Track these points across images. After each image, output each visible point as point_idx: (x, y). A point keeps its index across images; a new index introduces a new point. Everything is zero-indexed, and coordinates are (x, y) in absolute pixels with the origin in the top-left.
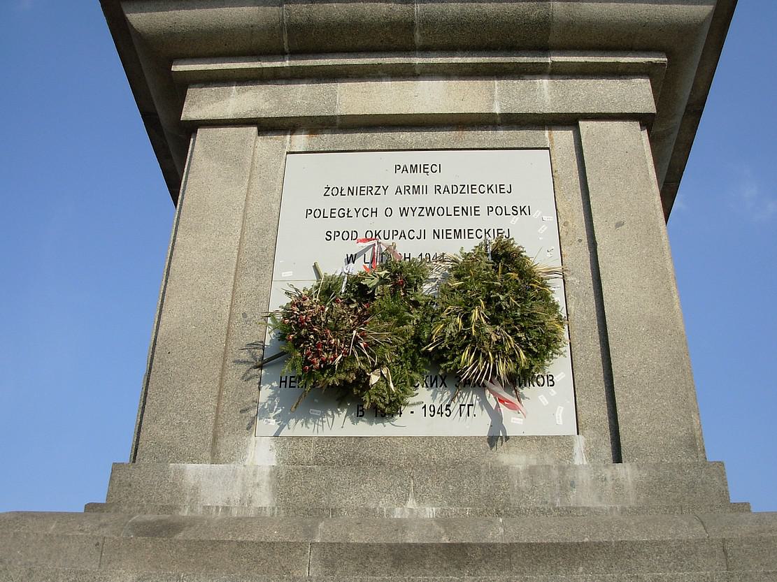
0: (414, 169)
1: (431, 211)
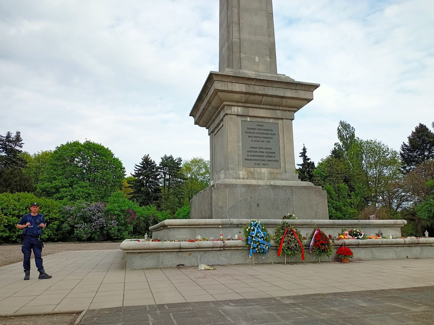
1: (262, 133)
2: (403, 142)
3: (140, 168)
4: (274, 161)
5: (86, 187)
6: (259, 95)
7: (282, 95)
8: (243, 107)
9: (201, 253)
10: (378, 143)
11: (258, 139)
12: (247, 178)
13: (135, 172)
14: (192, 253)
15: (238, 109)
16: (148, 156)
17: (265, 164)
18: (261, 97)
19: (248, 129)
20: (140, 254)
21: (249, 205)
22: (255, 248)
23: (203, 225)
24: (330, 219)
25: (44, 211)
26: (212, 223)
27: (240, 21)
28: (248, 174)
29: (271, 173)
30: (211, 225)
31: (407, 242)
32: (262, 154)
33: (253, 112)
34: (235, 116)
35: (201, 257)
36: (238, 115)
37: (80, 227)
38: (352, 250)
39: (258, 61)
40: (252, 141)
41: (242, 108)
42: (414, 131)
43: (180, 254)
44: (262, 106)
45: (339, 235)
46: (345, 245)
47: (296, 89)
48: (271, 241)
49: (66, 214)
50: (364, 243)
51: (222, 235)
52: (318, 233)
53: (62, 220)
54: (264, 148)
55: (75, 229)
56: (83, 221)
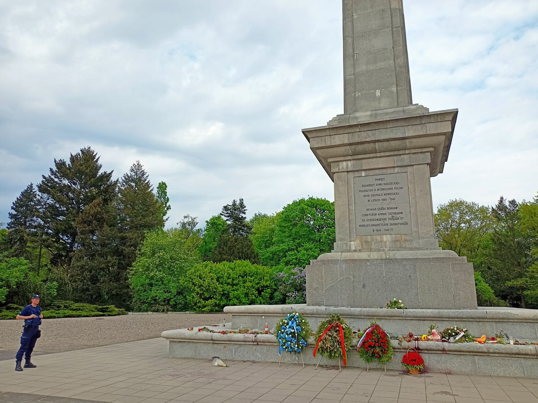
0: (379, 179)
5: (311, 249)
6: (369, 142)
8: (355, 161)
9: (236, 347)
11: (376, 198)
12: (359, 250)
14: (227, 345)
15: (347, 165)
17: (388, 230)
18: (372, 145)
20: (180, 343)
21: (351, 286)
23: (264, 313)
24: (480, 304)
25: (256, 278)
26: (271, 312)
27: (355, 51)
28: (362, 245)
30: (271, 313)
32: (384, 217)
34: (344, 173)
35: (236, 351)
36: (348, 172)
37: (291, 296)
38: (425, 357)
39: (380, 95)
40: (369, 201)
41: (352, 162)
43: (215, 345)
44: (378, 155)
47: (422, 123)
48: (310, 338)
49: (278, 281)
50: (453, 349)
51: (267, 327)
52: (372, 330)
53: (275, 287)
54: (386, 209)
55: (287, 298)
56: (295, 289)
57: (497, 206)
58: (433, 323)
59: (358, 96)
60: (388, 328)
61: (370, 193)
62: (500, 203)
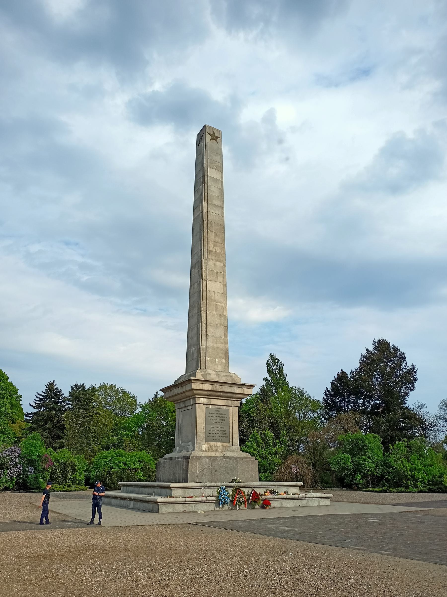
2: (326, 387)
3: (43, 398)
4: (226, 437)
6: (219, 392)
7: (233, 392)
10: (302, 390)
13: (35, 403)
14: (190, 504)
16: (54, 382)
19: (210, 413)
21: (210, 471)
22: (223, 501)
24: (260, 481)
26: (195, 486)
29: (223, 446)
31: (300, 497)
33: (214, 402)
35: (194, 507)
38: (271, 502)
40: (212, 422)
41: (206, 399)
42: (336, 377)
44: (219, 398)
45: (265, 492)
46: (267, 499)
50: (277, 498)
57: (152, 399)
58: (267, 488)
59: (208, 360)
60: (258, 491)
61: (213, 418)
62: (155, 397)
